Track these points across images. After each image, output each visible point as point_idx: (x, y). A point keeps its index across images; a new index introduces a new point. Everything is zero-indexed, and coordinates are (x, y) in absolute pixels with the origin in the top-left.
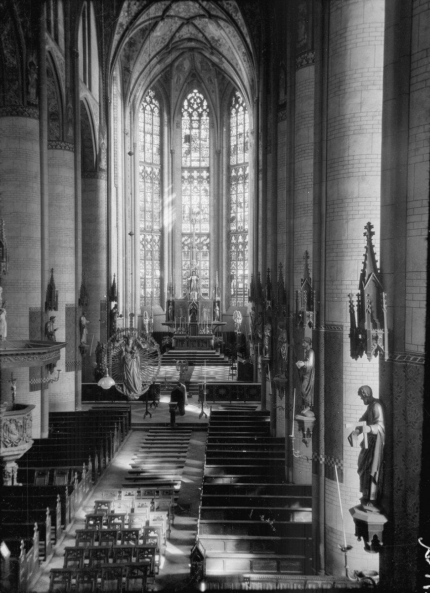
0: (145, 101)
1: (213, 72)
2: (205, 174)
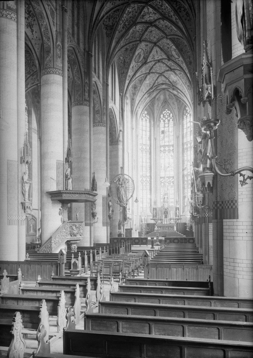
0: (143, 116)
1: (175, 99)
2: (171, 148)
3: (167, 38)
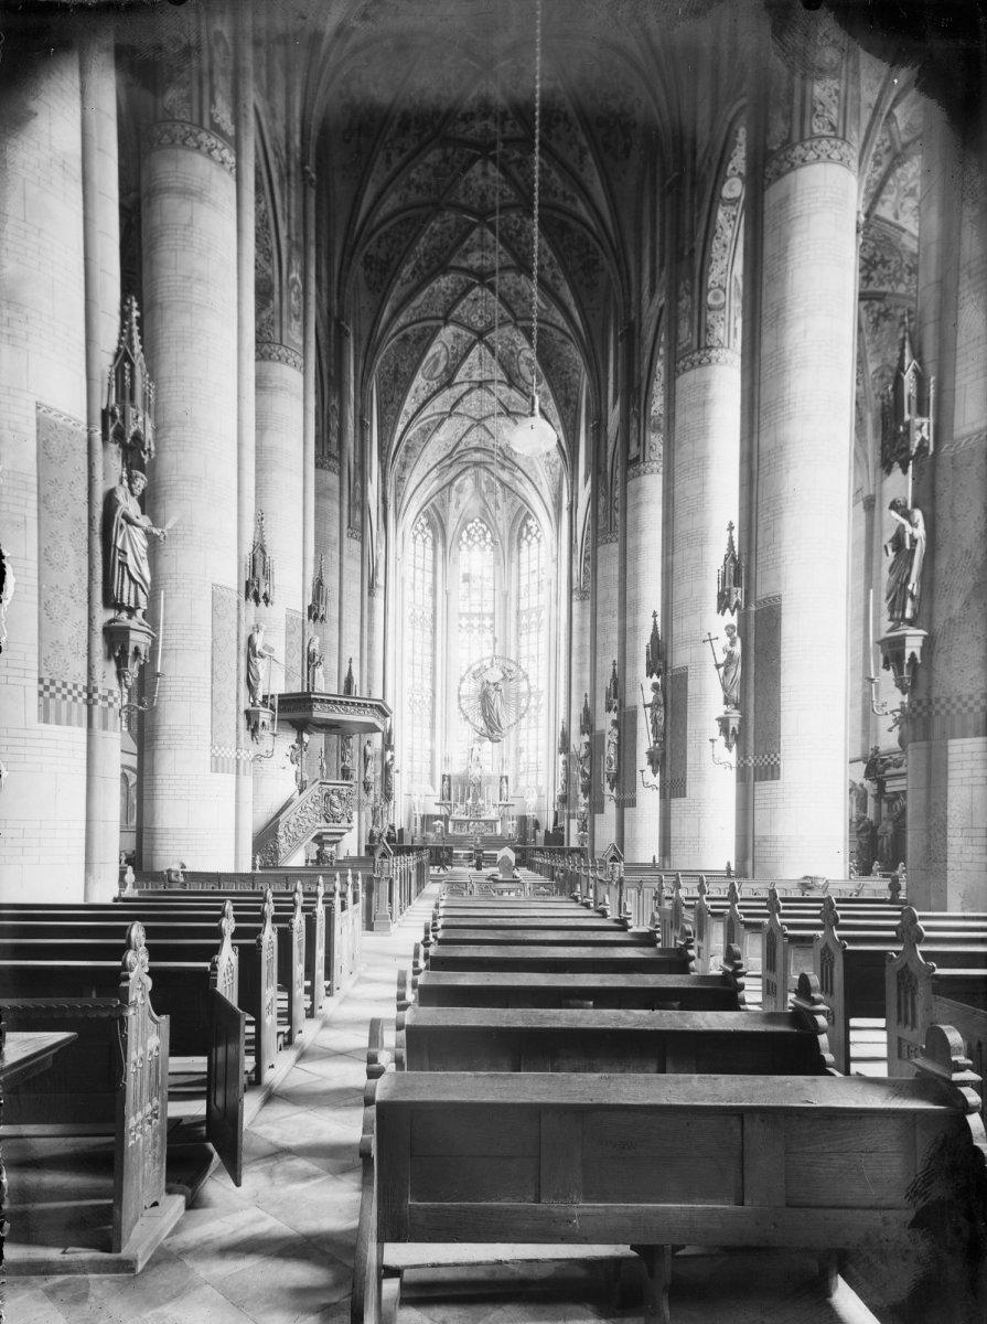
0: (416, 529)
3: (516, 326)
